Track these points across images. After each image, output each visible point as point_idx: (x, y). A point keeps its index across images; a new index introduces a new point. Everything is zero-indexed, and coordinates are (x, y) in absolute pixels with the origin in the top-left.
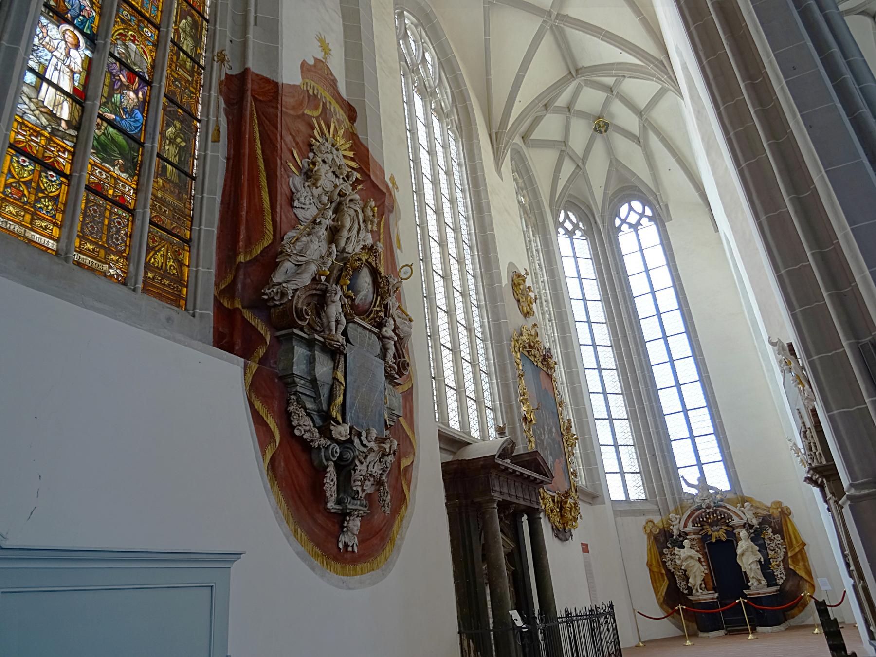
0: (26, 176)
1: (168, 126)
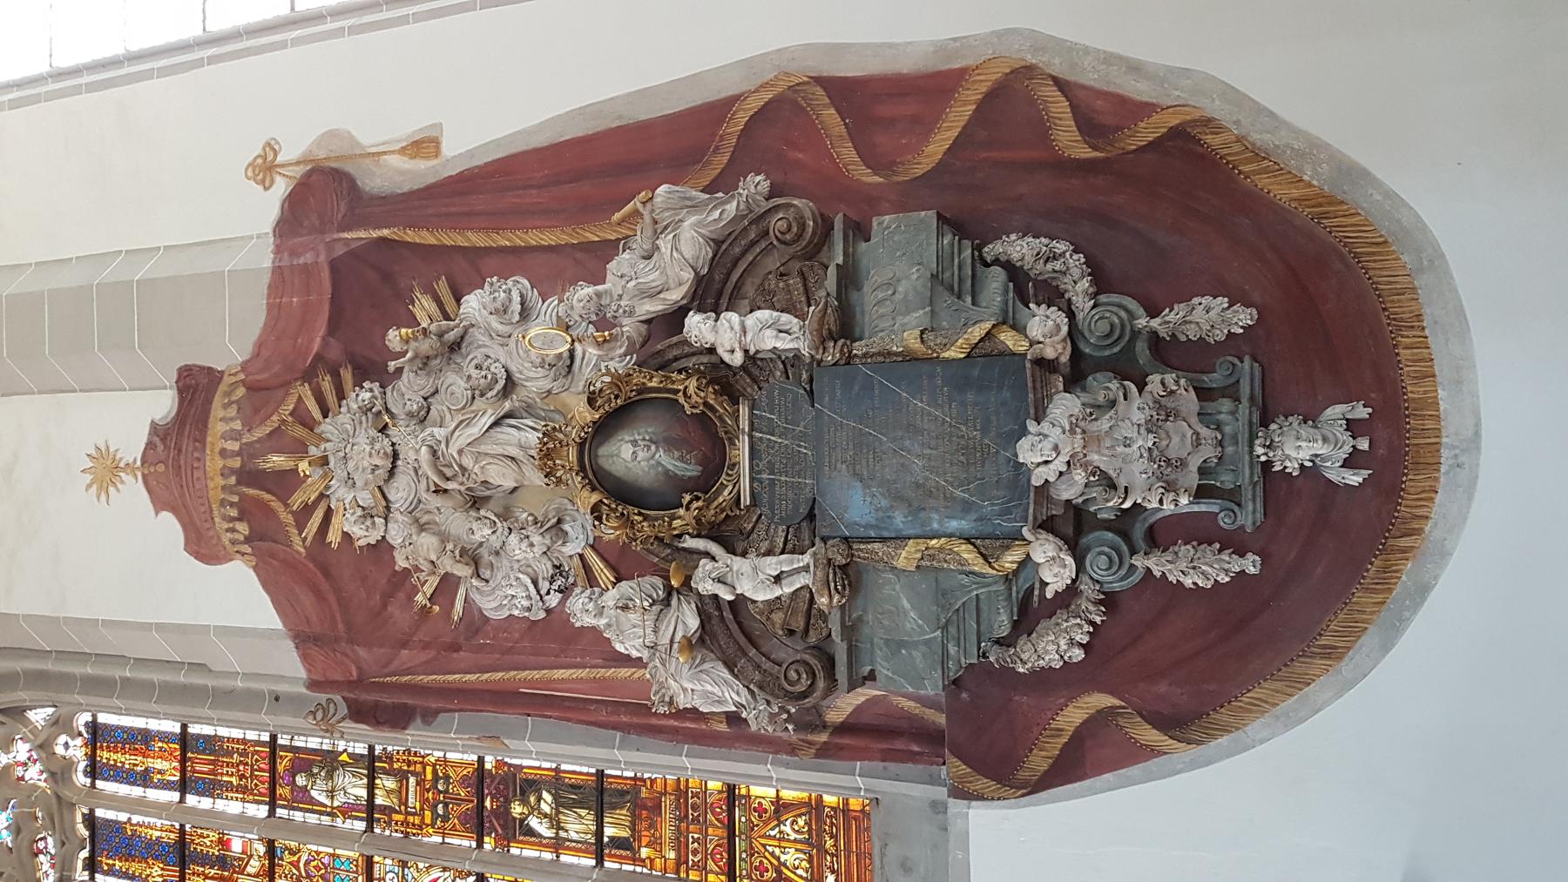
1: (531, 832)
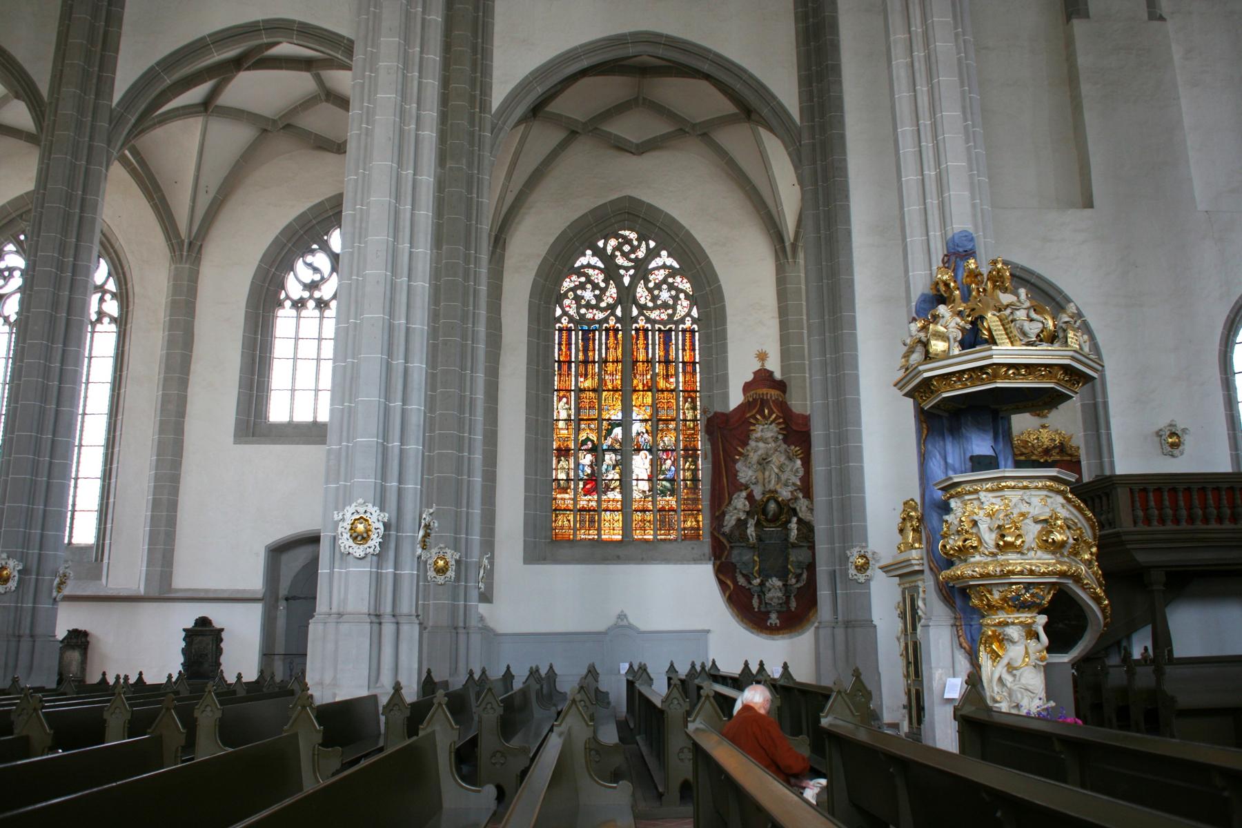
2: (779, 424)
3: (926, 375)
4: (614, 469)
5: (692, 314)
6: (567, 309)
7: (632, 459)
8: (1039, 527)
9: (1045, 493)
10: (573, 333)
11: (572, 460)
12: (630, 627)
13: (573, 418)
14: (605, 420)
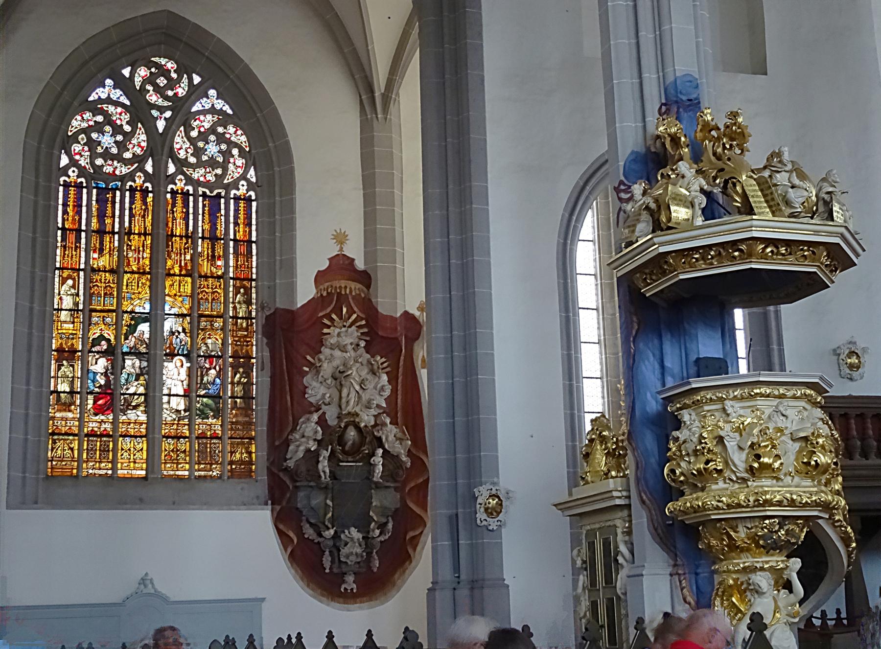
0: (172, 447)
2: (359, 327)
3: (662, 249)
4: (137, 379)
5: (248, 176)
6: (77, 157)
7: (162, 367)
8: (797, 446)
9: (803, 403)
10: (85, 191)
11: (78, 366)
12: (158, 595)
13: (81, 307)
14: (127, 312)
